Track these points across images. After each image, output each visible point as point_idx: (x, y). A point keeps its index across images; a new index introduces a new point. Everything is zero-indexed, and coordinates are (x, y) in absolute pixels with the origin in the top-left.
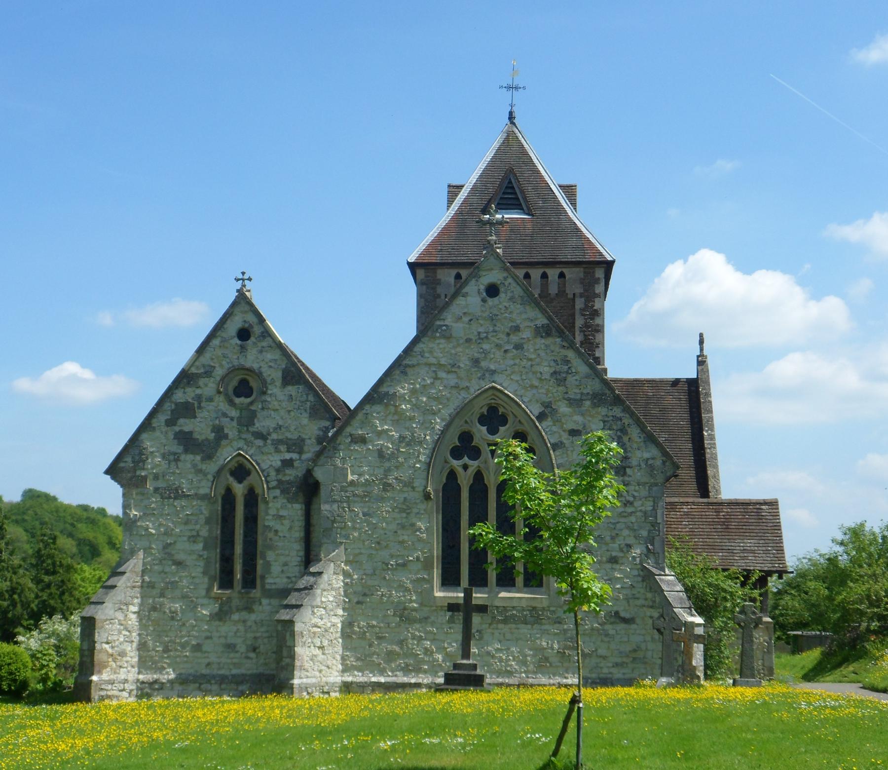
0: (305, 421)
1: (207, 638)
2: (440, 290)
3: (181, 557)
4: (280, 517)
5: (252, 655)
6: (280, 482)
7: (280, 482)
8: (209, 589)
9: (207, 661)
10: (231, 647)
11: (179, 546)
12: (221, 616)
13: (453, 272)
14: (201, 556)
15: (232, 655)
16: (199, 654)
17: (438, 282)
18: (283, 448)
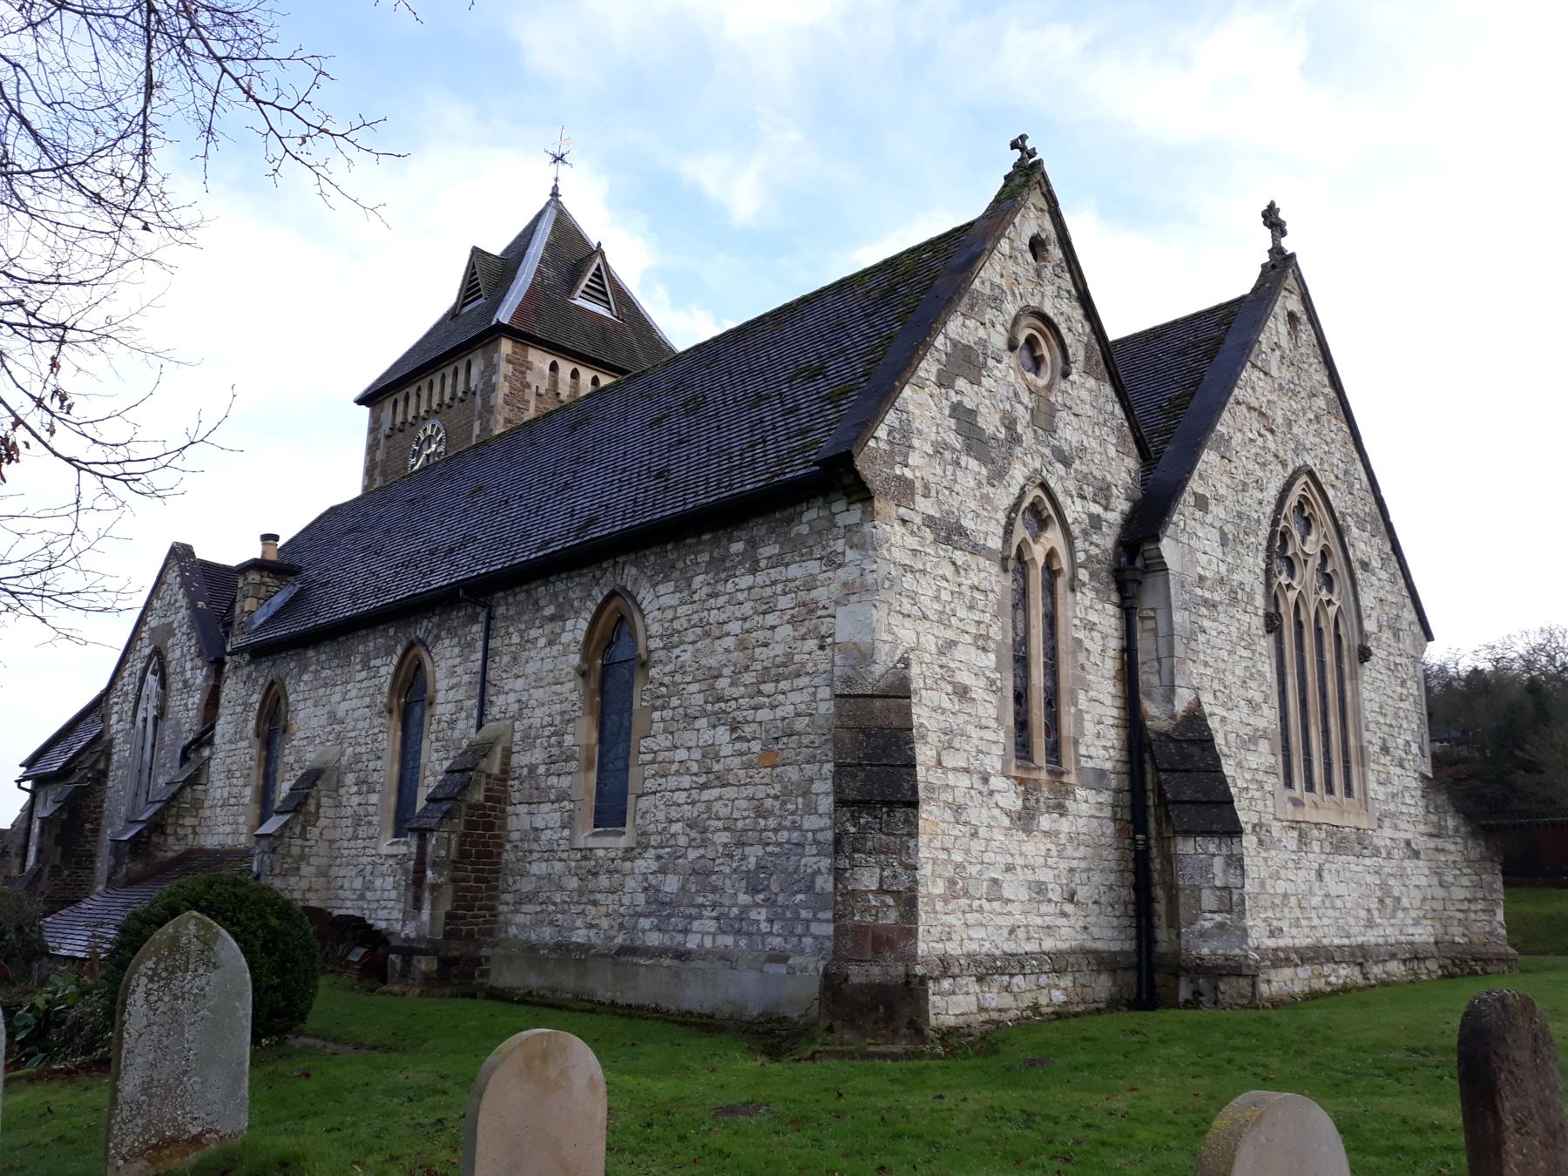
0: (1112, 452)
1: (1009, 868)
2: (530, 377)
3: (964, 677)
4: (1090, 627)
5: (1069, 908)
6: (1089, 557)
7: (1089, 557)
8: (1005, 764)
9: (1006, 922)
10: (1040, 889)
11: (960, 653)
12: (1024, 820)
13: (549, 359)
14: (993, 682)
15: (1045, 908)
16: (996, 905)
17: (529, 366)
18: (1088, 491)
